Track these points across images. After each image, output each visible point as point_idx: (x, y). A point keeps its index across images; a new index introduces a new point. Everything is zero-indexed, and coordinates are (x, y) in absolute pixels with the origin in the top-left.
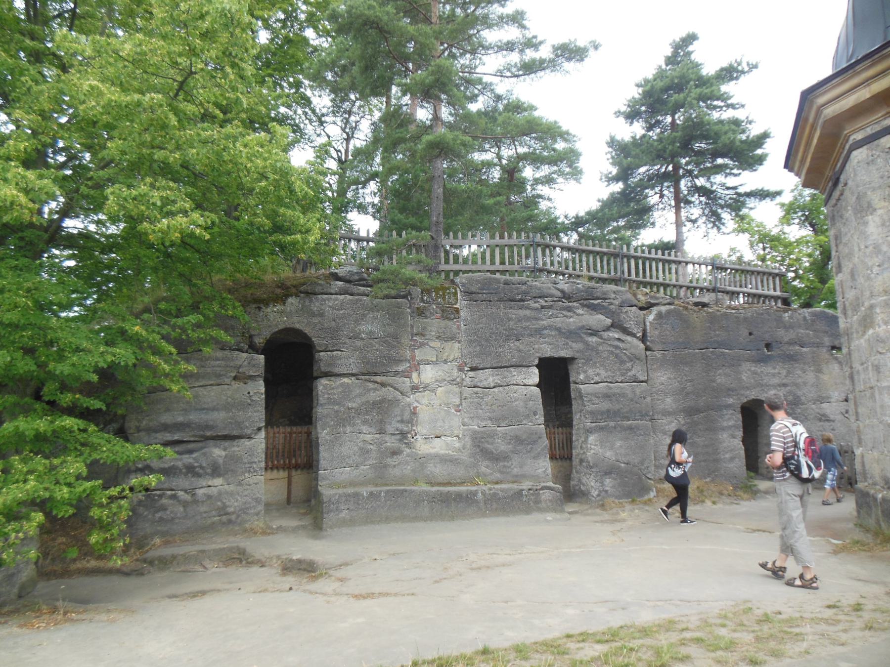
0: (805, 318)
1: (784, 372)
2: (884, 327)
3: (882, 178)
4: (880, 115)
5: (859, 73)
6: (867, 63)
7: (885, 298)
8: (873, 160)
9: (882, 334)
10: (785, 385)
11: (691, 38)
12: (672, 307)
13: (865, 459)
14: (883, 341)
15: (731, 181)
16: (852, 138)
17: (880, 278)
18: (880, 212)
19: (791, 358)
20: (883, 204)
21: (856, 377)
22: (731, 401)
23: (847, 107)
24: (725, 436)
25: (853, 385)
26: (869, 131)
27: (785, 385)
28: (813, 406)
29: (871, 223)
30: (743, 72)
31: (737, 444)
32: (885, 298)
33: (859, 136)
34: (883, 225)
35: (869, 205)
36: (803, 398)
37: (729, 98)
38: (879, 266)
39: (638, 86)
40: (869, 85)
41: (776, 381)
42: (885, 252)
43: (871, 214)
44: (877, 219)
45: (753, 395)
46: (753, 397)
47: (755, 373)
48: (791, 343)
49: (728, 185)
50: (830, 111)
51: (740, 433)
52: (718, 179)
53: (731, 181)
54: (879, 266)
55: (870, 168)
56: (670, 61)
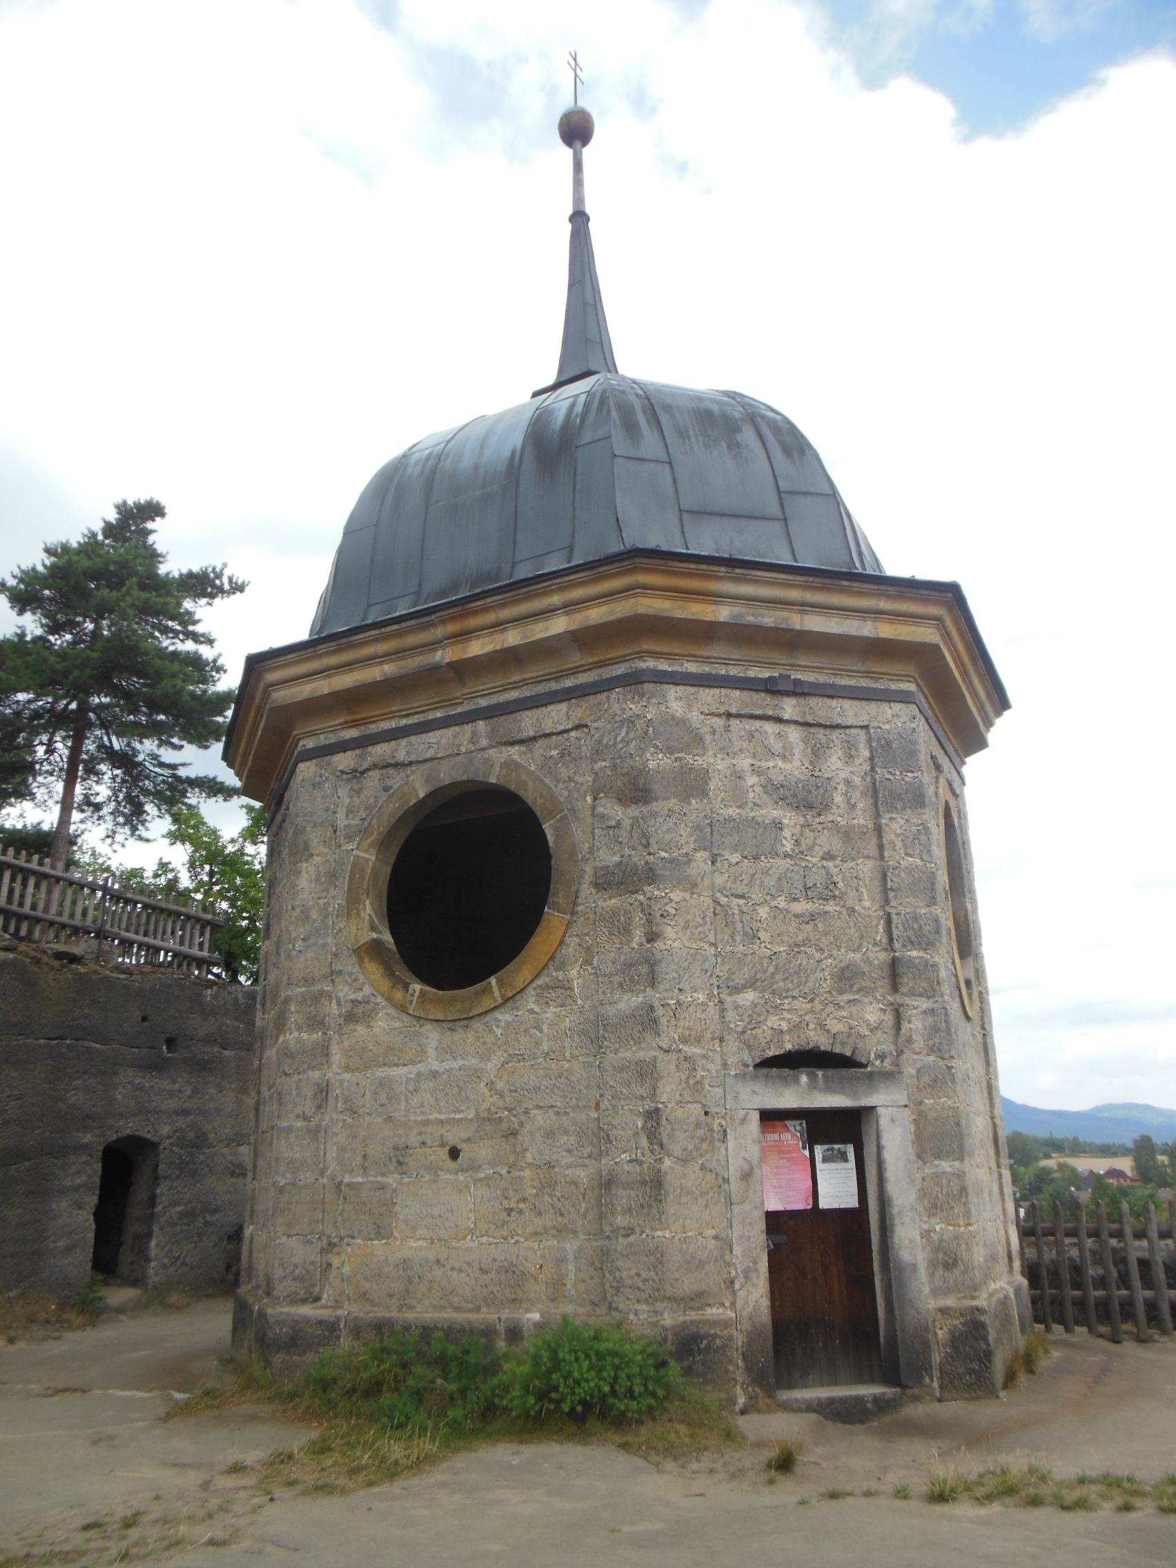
0: (236, 999)
1: (188, 1090)
3: (326, 811)
4: (337, 722)
5: (320, 656)
6: (332, 645)
8: (320, 783)
10: (186, 1113)
11: (153, 510)
12: (11, 956)
14: (292, 1057)
15: (168, 756)
16: (301, 744)
18: (317, 859)
19: (204, 1066)
21: (262, 1107)
22: (87, 1138)
23: (300, 698)
24: (64, 1204)
25: (257, 1121)
26: (323, 740)
27: (186, 1113)
28: (226, 1150)
29: (304, 873)
30: (221, 590)
31: (85, 1220)
32: (303, 989)
33: (310, 743)
34: (317, 880)
35: (306, 847)
36: (211, 1136)
37: (195, 622)
38: (303, 939)
39: (49, 551)
40: (329, 676)
41: (172, 1104)
42: (314, 922)
43: (307, 861)
44: (312, 869)
45: (129, 1127)
46: (128, 1132)
47: (140, 1088)
48: (209, 1040)
49: (163, 759)
50: (281, 696)
51: (93, 1200)
52: (147, 746)
53: (168, 756)
54: (303, 939)
56: (109, 529)
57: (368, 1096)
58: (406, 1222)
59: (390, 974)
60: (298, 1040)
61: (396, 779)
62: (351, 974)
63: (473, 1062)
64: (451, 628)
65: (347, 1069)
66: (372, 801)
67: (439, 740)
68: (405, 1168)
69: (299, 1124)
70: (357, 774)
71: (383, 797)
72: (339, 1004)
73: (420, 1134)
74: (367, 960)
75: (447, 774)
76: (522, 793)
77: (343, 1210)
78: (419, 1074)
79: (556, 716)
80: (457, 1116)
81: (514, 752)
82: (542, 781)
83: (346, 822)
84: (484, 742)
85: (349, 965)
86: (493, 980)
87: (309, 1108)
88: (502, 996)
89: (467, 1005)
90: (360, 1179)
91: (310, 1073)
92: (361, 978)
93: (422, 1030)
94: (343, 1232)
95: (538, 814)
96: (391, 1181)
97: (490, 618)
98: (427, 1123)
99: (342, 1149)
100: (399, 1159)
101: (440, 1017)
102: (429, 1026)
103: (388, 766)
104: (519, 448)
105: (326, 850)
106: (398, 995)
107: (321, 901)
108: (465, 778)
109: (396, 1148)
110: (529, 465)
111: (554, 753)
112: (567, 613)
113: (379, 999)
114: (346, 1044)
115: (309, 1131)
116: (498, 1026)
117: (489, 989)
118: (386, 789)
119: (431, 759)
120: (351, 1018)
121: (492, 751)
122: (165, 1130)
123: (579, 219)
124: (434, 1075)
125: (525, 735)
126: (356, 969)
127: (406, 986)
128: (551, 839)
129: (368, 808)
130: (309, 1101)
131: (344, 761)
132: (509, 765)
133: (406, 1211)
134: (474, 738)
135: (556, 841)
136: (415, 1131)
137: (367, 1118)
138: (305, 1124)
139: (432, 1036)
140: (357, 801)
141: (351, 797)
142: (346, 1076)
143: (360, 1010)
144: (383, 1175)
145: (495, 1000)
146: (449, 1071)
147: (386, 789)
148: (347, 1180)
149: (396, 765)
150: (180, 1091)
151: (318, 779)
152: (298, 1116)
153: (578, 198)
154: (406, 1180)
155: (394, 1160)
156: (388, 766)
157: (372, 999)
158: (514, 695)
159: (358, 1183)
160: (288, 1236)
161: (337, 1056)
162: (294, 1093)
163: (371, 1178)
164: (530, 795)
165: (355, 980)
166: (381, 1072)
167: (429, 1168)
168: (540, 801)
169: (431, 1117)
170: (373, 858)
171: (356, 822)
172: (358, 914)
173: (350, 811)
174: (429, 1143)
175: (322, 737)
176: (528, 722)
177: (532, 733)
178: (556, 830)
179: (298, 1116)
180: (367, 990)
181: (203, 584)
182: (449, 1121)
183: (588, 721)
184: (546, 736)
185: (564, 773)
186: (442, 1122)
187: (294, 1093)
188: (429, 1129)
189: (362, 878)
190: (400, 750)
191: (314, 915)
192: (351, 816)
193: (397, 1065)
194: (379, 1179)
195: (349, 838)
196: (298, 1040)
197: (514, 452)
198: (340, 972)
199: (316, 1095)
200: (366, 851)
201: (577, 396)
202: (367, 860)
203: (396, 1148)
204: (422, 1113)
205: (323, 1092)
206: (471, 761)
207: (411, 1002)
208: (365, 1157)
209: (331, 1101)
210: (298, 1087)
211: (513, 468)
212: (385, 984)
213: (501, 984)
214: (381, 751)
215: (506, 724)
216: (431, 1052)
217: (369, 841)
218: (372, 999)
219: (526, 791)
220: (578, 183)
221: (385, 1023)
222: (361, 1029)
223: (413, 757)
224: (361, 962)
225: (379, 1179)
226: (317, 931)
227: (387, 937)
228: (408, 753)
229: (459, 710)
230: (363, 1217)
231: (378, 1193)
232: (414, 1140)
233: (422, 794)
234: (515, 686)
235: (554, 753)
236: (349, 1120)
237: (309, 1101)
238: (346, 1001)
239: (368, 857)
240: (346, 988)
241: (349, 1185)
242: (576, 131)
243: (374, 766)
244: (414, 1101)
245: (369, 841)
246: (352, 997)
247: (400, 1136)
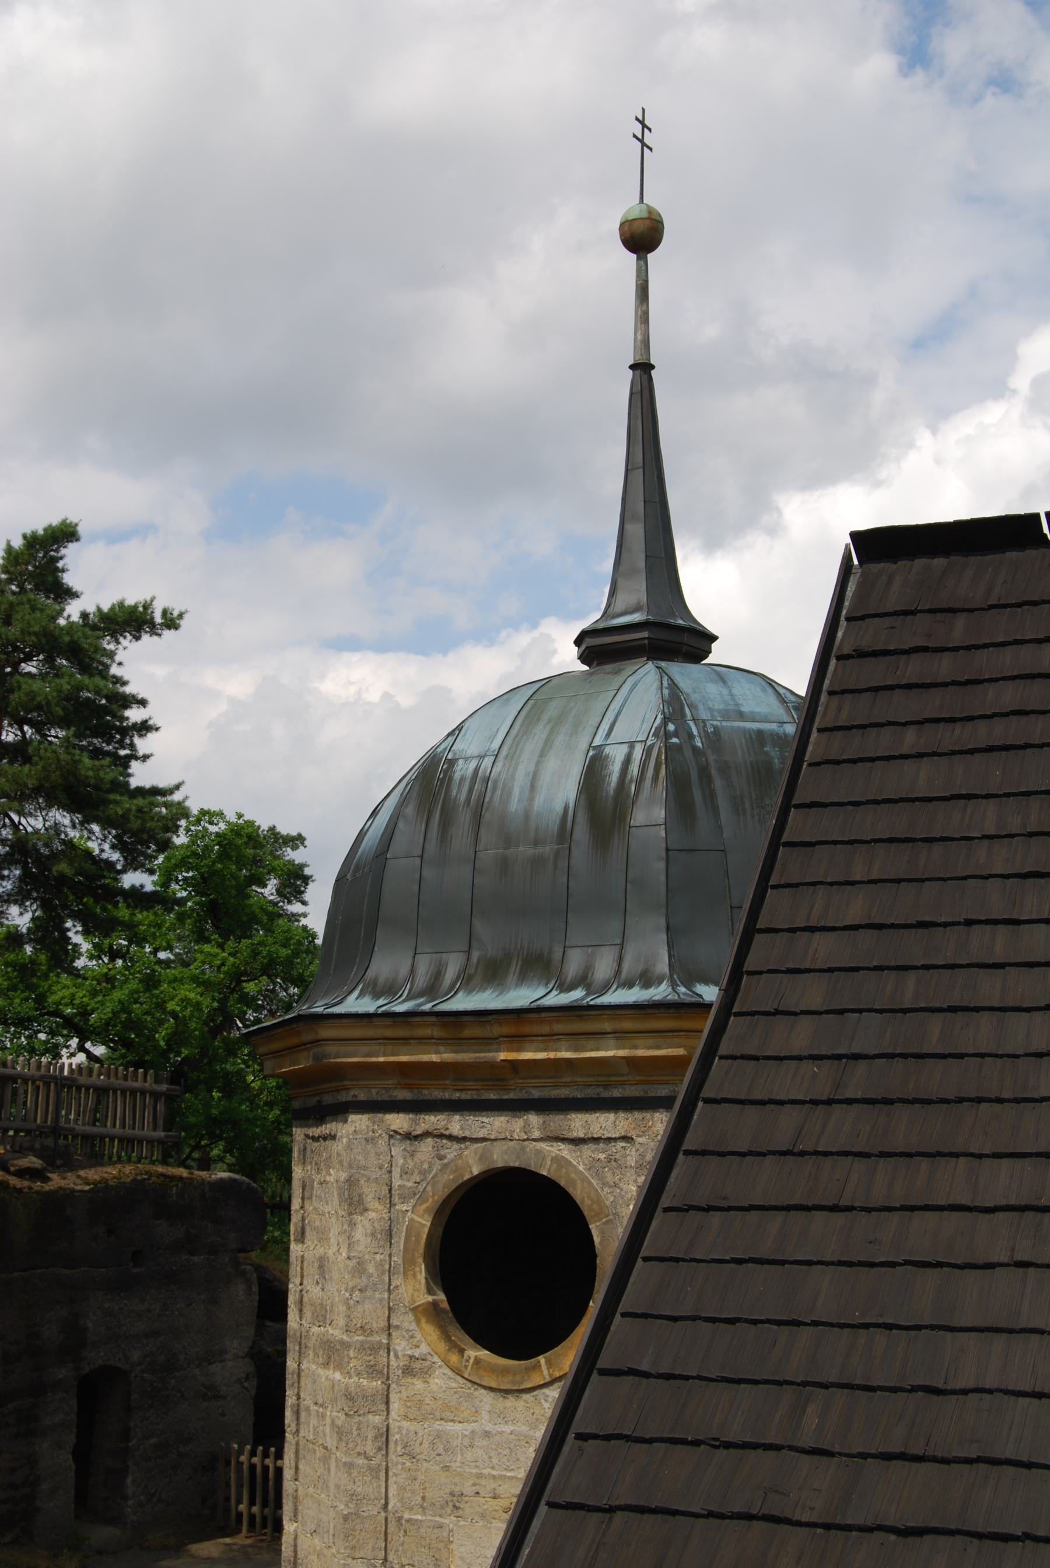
2: (356, 1379)
3: (381, 1168)
7: (361, 1338)
8: (373, 1139)
9: (352, 1389)
13: (299, 1542)
16: (352, 1093)
17: (360, 1308)
18: (372, 1215)
20: (376, 1205)
21: (303, 1414)
25: (298, 1424)
26: (375, 1094)
29: (359, 1226)
31: (65, 1459)
32: (361, 1338)
33: (362, 1096)
34: (373, 1235)
35: (361, 1201)
37: (125, 683)
40: (384, 1044)
42: (371, 1276)
43: (361, 1214)
55: (369, 1147)
57: (426, 1445)
58: (462, 1558)
59: (447, 1337)
60: (358, 1385)
61: (451, 1151)
62: (408, 1331)
63: (524, 1429)
64: (505, 1030)
65: (406, 1417)
66: (426, 1166)
67: (496, 1124)
68: (460, 1512)
69: (361, 1461)
70: (408, 1136)
71: (438, 1165)
72: (396, 1356)
73: (474, 1485)
74: (423, 1320)
75: (501, 1157)
76: (570, 1190)
77: (404, 1542)
78: (473, 1432)
79: (603, 1123)
80: (508, 1474)
81: (564, 1150)
82: (590, 1183)
83: (400, 1182)
84: (536, 1134)
85: (405, 1321)
86: (542, 1359)
87: (370, 1448)
88: (550, 1375)
89: (518, 1378)
90: (419, 1517)
91: (370, 1416)
92: (419, 1336)
93: (476, 1393)
94: (404, 1561)
95: (586, 1213)
96: (447, 1521)
97: (545, 1029)
98: (480, 1476)
99: (402, 1488)
100: (455, 1503)
101: (494, 1385)
102: (483, 1391)
103: (442, 1136)
104: (571, 805)
105: (381, 1208)
106: (454, 1358)
107: (378, 1257)
108: (517, 1165)
109: (452, 1494)
110: (581, 833)
111: (602, 1156)
112: (617, 1038)
113: (436, 1359)
114: (404, 1395)
115: (370, 1469)
116: (546, 1401)
117: (537, 1367)
118: (441, 1158)
119: (484, 1140)
120: (408, 1371)
121: (543, 1145)
122: (135, 1356)
123: (643, 368)
124: (487, 1434)
125: (575, 1135)
126: (413, 1326)
127: (462, 1351)
128: (597, 1239)
129: (423, 1173)
130: (369, 1442)
131: (398, 1121)
132: (558, 1160)
133: (462, 1549)
134: (526, 1128)
135: (601, 1242)
136: (471, 1482)
137: (425, 1464)
138: (366, 1462)
139: (486, 1399)
140: (411, 1164)
141: (405, 1159)
142: (405, 1424)
143: (417, 1365)
144: (440, 1516)
145: (544, 1378)
146: (501, 1433)
147: (441, 1158)
148: (406, 1516)
149: (451, 1138)
150: (149, 1311)
151: (371, 1133)
152: (359, 1454)
153: (644, 344)
154: (462, 1523)
155: (451, 1504)
156: (442, 1136)
157: (429, 1357)
158: (563, 1093)
159: (417, 1520)
160: (354, 1559)
161: (395, 1406)
162: (355, 1433)
163: (429, 1518)
164: (578, 1193)
165: (412, 1337)
166: (438, 1426)
167: (483, 1516)
168: (588, 1202)
169: (486, 1471)
170: (429, 1224)
171: (410, 1184)
172: (414, 1275)
173: (404, 1172)
174: (482, 1494)
175: (374, 1091)
176: (578, 1123)
177: (581, 1135)
178: (602, 1232)
179: (359, 1454)
180: (424, 1349)
181: (133, 621)
182: (501, 1477)
183: (632, 1134)
184: (596, 1140)
185: (609, 1177)
186: (494, 1477)
187: (355, 1433)
188: (483, 1482)
189: (418, 1241)
190: (456, 1124)
191: (371, 1269)
192: (405, 1177)
193: (453, 1421)
194: (437, 1519)
195: (404, 1199)
196: (358, 1385)
197: (566, 809)
198: (397, 1327)
199: (376, 1438)
200: (422, 1216)
201: (632, 745)
202: (424, 1225)
203: (452, 1494)
204: (477, 1467)
205: (385, 1435)
206: (523, 1149)
207: (466, 1367)
208: (423, 1498)
209: (391, 1445)
210: (358, 1429)
211: (564, 833)
212: (442, 1346)
213: (550, 1364)
214: (431, 1121)
215: (558, 1122)
216: (485, 1415)
217: (425, 1206)
218: (429, 1357)
219: (575, 1188)
220: (643, 318)
221: (442, 1381)
222: (419, 1384)
223: (467, 1134)
224: (418, 1321)
225: (437, 1519)
226: (375, 1285)
227: (441, 1296)
228: (462, 1128)
229: (511, 1096)
230: (423, 1550)
231: (436, 1531)
232: (468, 1489)
233: (476, 1172)
234: (566, 1085)
235: (602, 1156)
236: (408, 1464)
237: (369, 1442)
238: (404, 1355)
239: (419, 1219)
240: (404, 1343)
241: (408, 1521)
242: (642, 237)
243: (427, 1134)
244: (469, 1455)
245: (425, 1206)
246: (409, 1352)
247: (456, 1484)
